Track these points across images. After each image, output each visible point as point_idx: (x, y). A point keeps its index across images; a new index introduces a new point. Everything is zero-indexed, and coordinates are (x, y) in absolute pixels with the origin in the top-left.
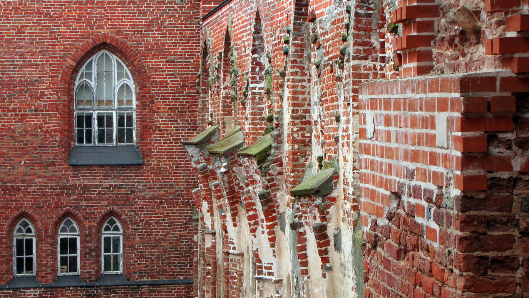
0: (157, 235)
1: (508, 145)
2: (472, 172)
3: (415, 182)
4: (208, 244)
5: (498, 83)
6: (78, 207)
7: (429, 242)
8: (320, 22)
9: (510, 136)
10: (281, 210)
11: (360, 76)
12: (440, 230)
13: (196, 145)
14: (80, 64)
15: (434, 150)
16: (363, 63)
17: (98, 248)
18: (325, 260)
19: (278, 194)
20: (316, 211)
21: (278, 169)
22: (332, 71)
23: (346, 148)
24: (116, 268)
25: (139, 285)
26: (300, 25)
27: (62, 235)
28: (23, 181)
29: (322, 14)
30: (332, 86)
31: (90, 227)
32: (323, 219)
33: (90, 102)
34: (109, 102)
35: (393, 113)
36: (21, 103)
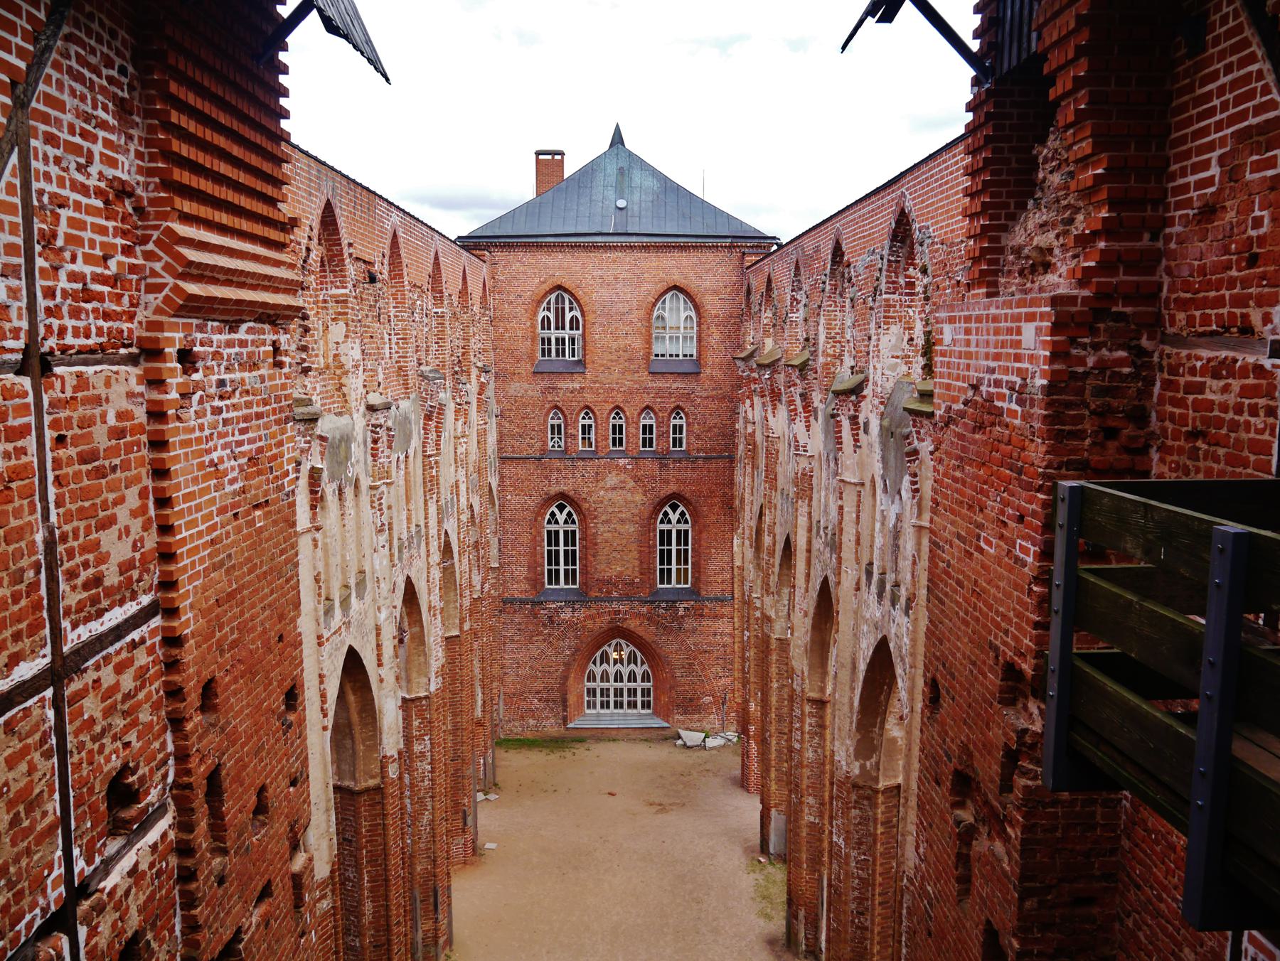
0: (710, 423)
1: (1084, 346)
2: (1057, 367)
3: (996, 376)
4: (750, 430)
9: (1086, 340)
10: (815, 405)
11: (889, 306)
13: (743, 359)
14: (657, 300)
17: (668, 432)
18: (856, 440)
24: (681, 446)
27: (643, 422)
32: (856, 411)
33: (664, 328)
34: (678, 328)
35: (973, 325)
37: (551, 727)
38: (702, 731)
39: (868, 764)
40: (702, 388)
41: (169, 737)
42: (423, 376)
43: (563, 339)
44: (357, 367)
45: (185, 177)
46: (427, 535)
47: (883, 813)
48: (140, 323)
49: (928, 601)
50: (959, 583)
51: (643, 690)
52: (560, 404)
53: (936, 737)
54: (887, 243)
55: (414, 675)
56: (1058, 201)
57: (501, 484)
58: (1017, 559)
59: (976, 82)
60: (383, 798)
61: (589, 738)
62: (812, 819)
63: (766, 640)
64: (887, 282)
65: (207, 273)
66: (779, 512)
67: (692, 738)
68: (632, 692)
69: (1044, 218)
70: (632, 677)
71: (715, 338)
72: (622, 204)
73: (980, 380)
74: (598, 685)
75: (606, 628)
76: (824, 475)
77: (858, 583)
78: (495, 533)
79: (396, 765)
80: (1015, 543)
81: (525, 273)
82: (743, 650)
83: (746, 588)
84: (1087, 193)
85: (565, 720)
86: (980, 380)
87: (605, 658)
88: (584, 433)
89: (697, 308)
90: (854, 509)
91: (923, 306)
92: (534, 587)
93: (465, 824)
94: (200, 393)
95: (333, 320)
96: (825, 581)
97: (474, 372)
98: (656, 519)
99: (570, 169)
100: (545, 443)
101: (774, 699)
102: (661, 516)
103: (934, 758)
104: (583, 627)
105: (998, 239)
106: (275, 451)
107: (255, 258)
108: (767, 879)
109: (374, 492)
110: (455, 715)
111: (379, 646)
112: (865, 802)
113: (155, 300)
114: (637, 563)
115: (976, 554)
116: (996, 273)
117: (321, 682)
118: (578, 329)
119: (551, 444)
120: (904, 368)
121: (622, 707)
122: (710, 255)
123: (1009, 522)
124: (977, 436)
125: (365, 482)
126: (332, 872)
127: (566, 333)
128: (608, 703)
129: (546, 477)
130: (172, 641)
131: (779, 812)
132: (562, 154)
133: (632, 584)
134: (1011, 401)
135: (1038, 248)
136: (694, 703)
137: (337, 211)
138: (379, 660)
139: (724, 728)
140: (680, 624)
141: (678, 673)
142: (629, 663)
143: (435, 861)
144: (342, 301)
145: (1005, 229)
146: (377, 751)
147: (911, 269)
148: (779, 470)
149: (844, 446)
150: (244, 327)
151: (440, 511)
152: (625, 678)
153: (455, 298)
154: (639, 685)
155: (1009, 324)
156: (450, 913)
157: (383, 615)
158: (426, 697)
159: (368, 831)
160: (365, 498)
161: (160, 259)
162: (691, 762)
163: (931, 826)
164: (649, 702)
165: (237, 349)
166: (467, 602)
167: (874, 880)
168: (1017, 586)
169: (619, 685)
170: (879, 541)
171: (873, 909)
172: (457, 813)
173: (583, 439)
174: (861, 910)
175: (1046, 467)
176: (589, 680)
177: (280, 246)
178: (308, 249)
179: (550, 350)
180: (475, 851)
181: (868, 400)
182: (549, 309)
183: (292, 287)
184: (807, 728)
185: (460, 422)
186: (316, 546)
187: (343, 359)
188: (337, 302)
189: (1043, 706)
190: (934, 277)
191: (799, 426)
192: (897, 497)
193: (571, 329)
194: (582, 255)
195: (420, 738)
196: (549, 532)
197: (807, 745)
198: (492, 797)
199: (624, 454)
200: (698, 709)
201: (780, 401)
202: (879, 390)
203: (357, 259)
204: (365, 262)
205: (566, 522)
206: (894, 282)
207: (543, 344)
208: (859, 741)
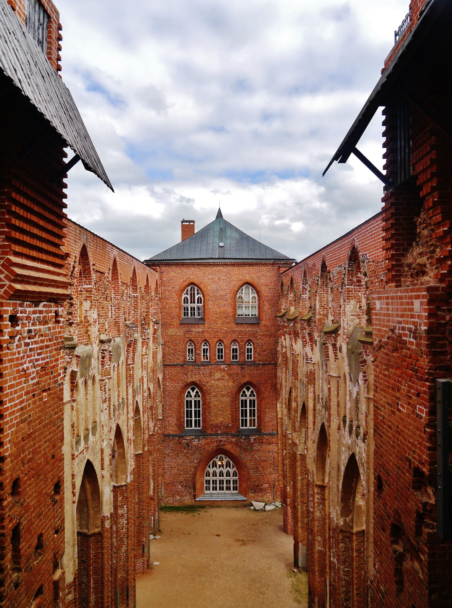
0: (265, 348)
1: (444, 311)
2: (431, 321)
3: (402, 325)
4: (284, 351)
5: (440, 289)
7: (409, 346)
8: (332, 273)
9: (445, 308)
10: (315, 338)
11: (350, 291)
12: (416, 342)
14: (239, 289)
16: (350, 287)
17: (245, 352)
18: (336, 356)
19: (315, 333)
20: (332, 339)
21: (314, 324)
22: (337, 290)
23: (344, 316)
24: (251, 359)
25: (259, 364)
26: (323, 274)
27: (232, 347)
28: (220, 329)
29: (333, 270)
30: (338, 295)
31: (242, 345)
32: (335, 341)
33: (242, 302)
34: (249, 302)
35: (390, 301)
36: (220, 302)
37: (188, 500)
38: (263, 502)
39: (348, 519)
40: (260, 331)
42: (127, 326)
43: (194, 308)
44: (95, 322)
45: (17, 235)
47: (356, 545)
49: (374, 436)
50: (389, 427)
51: (233, 481)
52: (192, 339)
53: (381, 506)
54: (347, 262)
56: (427, 242)
58: (418, 415)
59: (385, 189)
62: (320, 548)
64: (348, 280)
65: (25, 279)
66: (299, 391)
67: (258, 505)
68: (228, 482)
69: (421, 250)
70: (228, 474)
71: (266, 307)
72: (222, 244)
73: (395, 327)
74: (211, 478)
75: (215, 448)
76: (321, 373)
77: (339, 426)
78: (161, 402)
79: (109, 521)
80: (416, 407)
81: (176, 277)
82: (283, 460)
83: (284, 428)
84: (440, 239)
85: (195, 497)
86: (395, 327)
87: (215, 465)
88: (204, 353)
89: (258, 293)
90: (336, 389)
91: (365, 291)
92: (179, 428)
93: (144, 552)
94: (19, 336)
95: (85, 300)
96: (323, 425)
97: (152, 324)
98: (239, 394)
100: (185, 358)
101: (299, 485)
102: (241, 393)
103: (381, 517)
104: (204, 448)
105: (400, 260)
106: (54, 363)
107: (48, 272)
108: (298, 581)
109: (102, 382)
110: (139, 494)
111: (102, 459)
112: (347, 540)
114: (230, 416)
115: (397, 413)
116: (399, 276)
117: (73, 478)
118: (201, 303)
119: (188, 358)
120: (358, 321)
122: (264, 268)
124: (395, 354)
125: (98, 378)
127: (196, 305)
128: (216, 487)
129: (186, 374)
131: (303, 545)
132: (194, 222)
133: (228, 427)
134: (410, 337)
135: (419, 264)
136: (259, 487)
137: (88, 249)
140: (252, 447)
141: (251, 472)
142: (226, 467)
143: (127, 572)
145: (403, 255)
147: (359, 274)
148: (299, 370)
149: (330, 358)
150: (42, 304)
151: (134, 391)
152: (225, 475)
153: (143, 289)
154: (232, 478)
155: (407, 300)
157: (105, 444)
158: (125, 485)
159: (93, 556)
160: (97, 385)
161: (3, 273)
162: (258, 518)
163: (381, 553)
164: (237, 487)
165: (38, 315)
166: (146, 436)
167: (353, 581)
168: (418, 429)
169: (221, 478)
170: (348, 405)
171: (353, 598)
172: (139, 546)
173: (204, 355)
174: (347, 598)
175: (429, 369)
176: (206, 476)
177: (60, 266)
178: (74, 267)
179: (188, 313)
180: (149, 566)
181: (341, 336)
182: (187, 294)
183: (65, 285)
184: (316, 500)
185: (144, 348)
188: (87, 291)
190: (370, 277)
191: (308, 349)
192: (357, 383)
193: (198, 303)
194: (203, 268)
195: (122, 507)
196: (187, 401)
197: (316, 509)
198: (158, 537)
199: (223, 363)
200: (261, 490)
201: (298, 337)
202: (346, 331)
203: (97, 271)
204: (100, 272)
205: (195, 396)
206: (351, 280)
207: (185, 310)
208: (342, 507)
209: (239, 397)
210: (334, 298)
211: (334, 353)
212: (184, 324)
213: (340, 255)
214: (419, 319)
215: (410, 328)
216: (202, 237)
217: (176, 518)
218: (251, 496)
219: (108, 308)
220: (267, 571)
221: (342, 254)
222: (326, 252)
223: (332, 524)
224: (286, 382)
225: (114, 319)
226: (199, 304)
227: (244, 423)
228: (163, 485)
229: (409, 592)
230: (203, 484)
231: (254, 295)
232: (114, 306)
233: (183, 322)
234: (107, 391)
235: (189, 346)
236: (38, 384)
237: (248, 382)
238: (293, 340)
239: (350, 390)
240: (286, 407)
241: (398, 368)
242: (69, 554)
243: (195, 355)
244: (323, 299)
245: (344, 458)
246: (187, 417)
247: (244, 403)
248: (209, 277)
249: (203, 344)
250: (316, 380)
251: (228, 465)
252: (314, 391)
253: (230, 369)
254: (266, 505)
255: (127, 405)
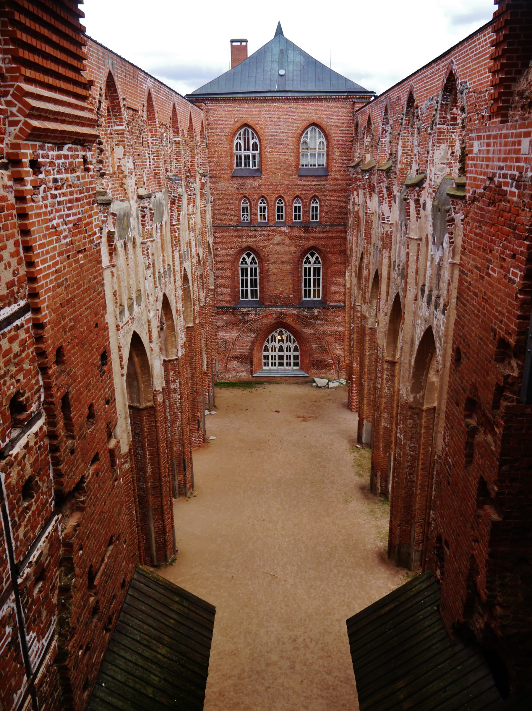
0: (334, 205)
4: (356, 209)
6: (301, 194)
7: (510, 198)
10: (395, 193)
11: (441, 132)
13: (353, 167)
14: (303, 132)
15: (519, 156)
17: (309, 210)
18: (418, 214)
19: (394, 187)
20: (415, 193)
24: (316, 219)
25: (325, 226)
27: (295, 205)
30: (426, 138)
32: (419, 196)
33: (307, 149)
34: (315, 149)
37: (244, 376)
38: (327, 379)
39: (418, 396)
40: (328, 185)
41: (40, 377)
42: (168, 178)
43: (249, 156)
44: (131, 173)
45: (26, 55)
46: (174, 270)
48: (7, 144)
49: (457, 304)
50: (475, 294)
51: (294, 356)
52: (247, 195)
53: (458, 380)
54: (441, 93)
55: (169, 347)
57: (215, 242)
58: (510, 280)
60: (155, 413)
61: (265, 382)
62: (386, 425)
63: (363, 329)
65: (43, 114)
66: (372, 256)
67: (321, 382)
68: (288, 357)
71: (336, 155)
72: (282, 72)
74: (270, 353)
75: (274, 322)
76: (399, 235)
77: (416, 297)
78: (212, 269)
79: (161, 395)
80: (509, 270)
81: (226, 116)
82: (350, 334)
83: (353, 300)
85: (252, 373)
86: (494, 175)
87: (273, 339)
88: (261, 212)
89: (327, 136)
90: (416, 254)
91: (461, 132)
92: (234, 299)
93: (199, 427)
94: (44, 186)
95: (116, 145)
96: (398, 295)
97: (198, 176)
98: (302, 261)
99: (251, 51)
100: (239, 218)
101: (367, 361)
102: (305, 260)
103: (456, 391)
105: (509, 87)
106: (88, 220)
107: (70, 105)
108: (360, 456)
109: (144, 246)
110: (192, 369)
111: (150, 331)
112: (416, 416)
113: (14, 130)
114: (291, 286)
115: (486, 277)
116: (507, 108)
117: (120, 351)
118: (257, 150)
120: (448, 170)
121: (283, 365)
122: (334, 104)
123: (507, 258)
124: (491, 208)
125: (139, 240)
126: (130, 449)
127: (250, 153)
128: (275, 363)
129: (240, 238)
130: (38, 326)
131: (368, 421)
132: (246, 41)
133: (288, 298)
134: (512, 186)
137: (115, 78)
138: (150, 339)
139: (339, 377)
140: (315, 320)
141: (314, 347)
142: (287, 342)
143: (183, 445)
144: (121, 134)
145: (515, 80)
146: (151, 387)
147: (455, 109)
148: (373, 232)
149: (411, 217)
150: (66, 147)
151: (180, 256)
152: (285, 350)
153: (186, 132)
154: (292, 354)
155: (514, 139)
156: (192, 472)
157: (151, 315)
158: (176, 360)
160: (139, 249)
161: (15, 105)
162: (320, 395)
163: (452, 427)
164: (298, 363)
165: (63, 160)
166: (197, 308)
167: (419, 457)
168: (509, 295)
169: (281, 353)
170: (429, 272)
171: (418, 472)
172: (194, 421)
173: (261, 215)
174: (411, 472)
176: (265, 351)
177: (84, 98)
178: (100, 102)
179: (241, 163)
180: (204, 441)
181: (426, 190)
182: (240, 138)
183: (92, 123)
184: (385, 377)
185: (191, 206)
186: (113, 276)
187: (123, 168)
188: (118, 134)
189: (520, 362)
191: (385, 206)
192: (441, 247)
193: (253, 150)
195: (174, 381)
196: (242, 269)
197: (384, 386)
198: (213, 412)
200: (325, 367)
201: (374, 192)
202: (433, 183)
204: (133, 110)
205: (251, 263)
206: (444, 118)
207: (237, 159)
208: (413, 383)
209: (302, 263)
210: (421, 142)
211: (416, 211)
212: (237, 177)
213: (432, 84)
214: (526, 163)
215: (513, 175)
216: (257, 62)
217: (231, 394)
218: (314, 373)
219: (145, 156)
220: (329, 447)
221: (435, 82)
222: (415, 80)
223: (401, 400)
224: (357, 247)
225: (154, 170)
226: (255, 152)
227: (307, 293)
228: (217, 360)
229: (478, 464)
230: (261, 361)
231: (321, 139)
232: (153, 154)
233: (236, 175)
234: (150, 256)
235: (243, 203)
236: (72, 244)
237: (312, 246)
238: (368, 196)
239: (432, 255)
240: (356, 276)
241: (494, 225)
242: (121, 426)
243: (251, 214)
244: (407, 144)
245: (420, 332)
246: (242, 287)
247: (307, 271)
248: (266, 116)
249: (260, 201)
250: (393, 244)
251: (288, 339)
252: (390, 257)
253: (291, 232)
254: (329, 381)
255: (174, 272)
